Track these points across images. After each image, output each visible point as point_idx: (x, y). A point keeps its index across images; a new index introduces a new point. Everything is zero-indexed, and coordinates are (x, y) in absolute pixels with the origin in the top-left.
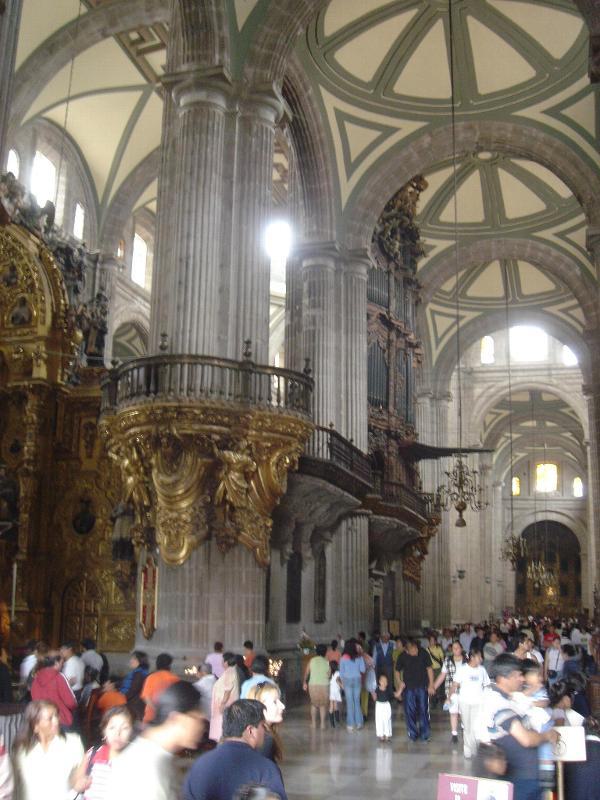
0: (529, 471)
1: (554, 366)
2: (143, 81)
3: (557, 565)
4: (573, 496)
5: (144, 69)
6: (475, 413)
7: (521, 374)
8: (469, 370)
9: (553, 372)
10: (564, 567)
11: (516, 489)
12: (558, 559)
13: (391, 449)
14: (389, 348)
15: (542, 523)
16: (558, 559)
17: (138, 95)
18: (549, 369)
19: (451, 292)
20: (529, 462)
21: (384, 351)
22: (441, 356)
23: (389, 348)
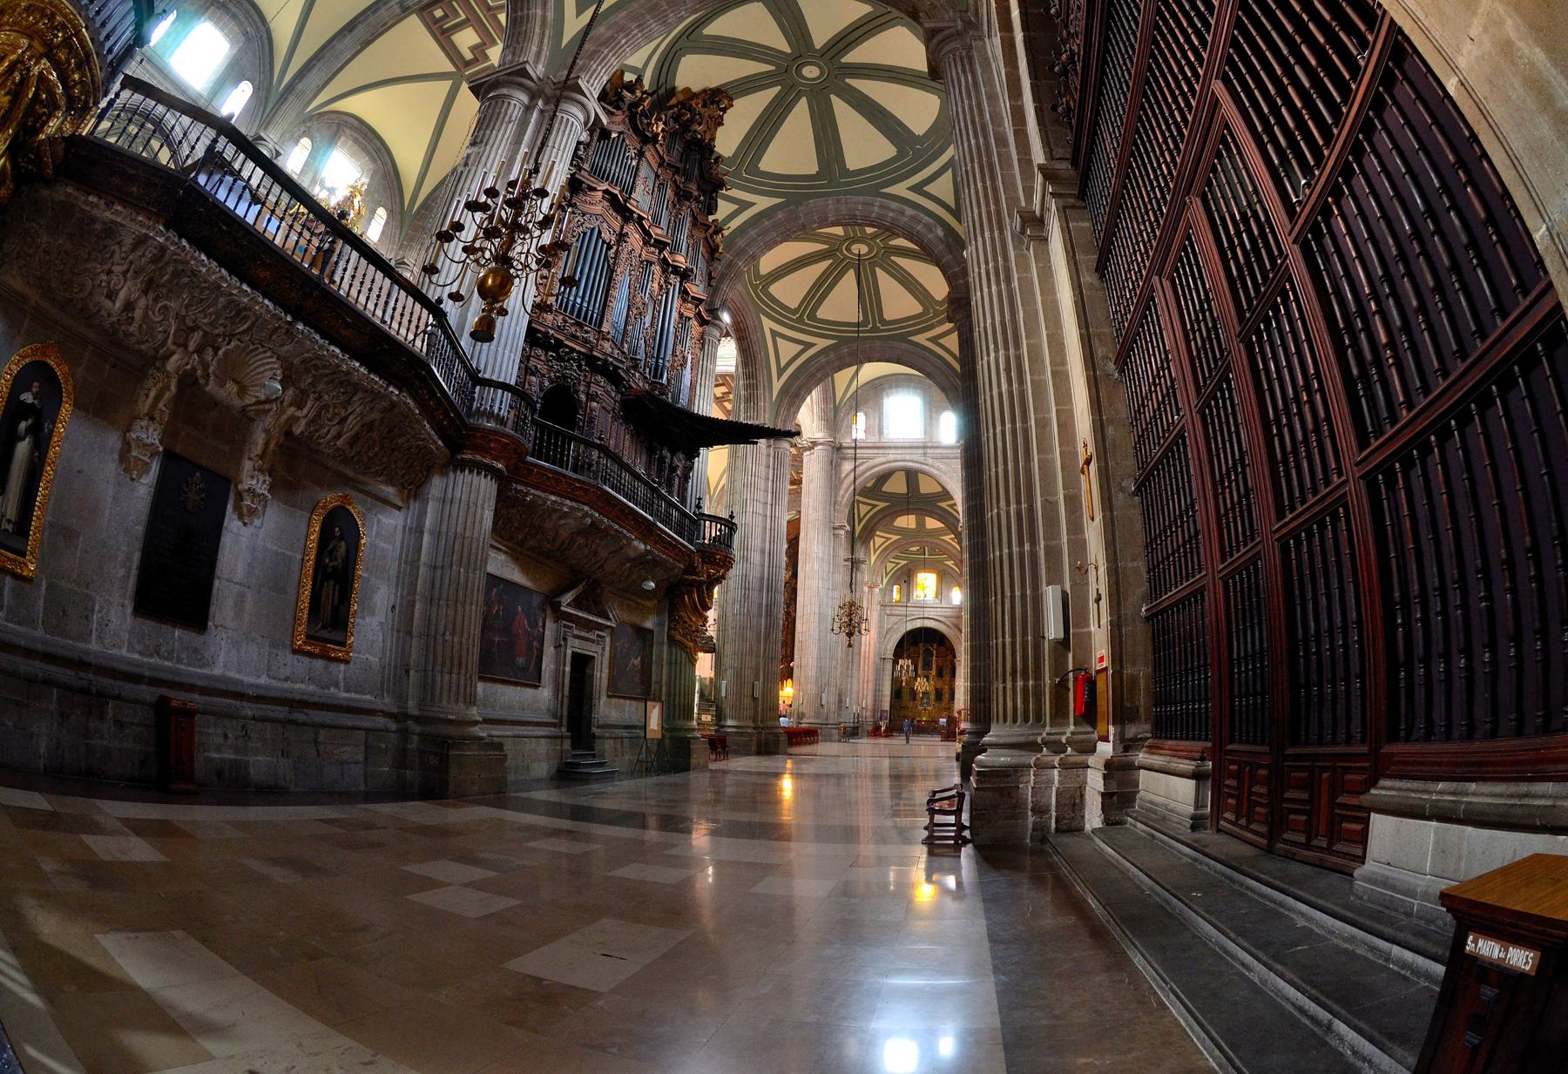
0: (909, 577)
1: (930, 444)
2: (452, 68)
3: (934, 672)
4: (951, 603)
5: (451, 51)
6: (842, 492)
7: (893, 451)
8: (838, 445)
9: (929, 451)
10: (940, 674)
11: (896, 596)
12: (934, 666)
13: (593, 388)
14: (618, 242)
15: (920, 630)
16: (934, 666)
17: (447, 84)
18: (924, 447)
19: (796, 311)
20: (909, 570)
21: (609, 247)
22: (785, 390)
23: (618, 242)
